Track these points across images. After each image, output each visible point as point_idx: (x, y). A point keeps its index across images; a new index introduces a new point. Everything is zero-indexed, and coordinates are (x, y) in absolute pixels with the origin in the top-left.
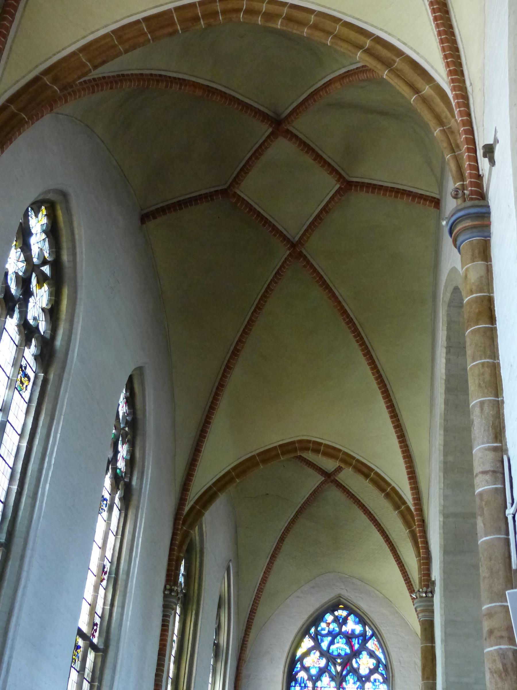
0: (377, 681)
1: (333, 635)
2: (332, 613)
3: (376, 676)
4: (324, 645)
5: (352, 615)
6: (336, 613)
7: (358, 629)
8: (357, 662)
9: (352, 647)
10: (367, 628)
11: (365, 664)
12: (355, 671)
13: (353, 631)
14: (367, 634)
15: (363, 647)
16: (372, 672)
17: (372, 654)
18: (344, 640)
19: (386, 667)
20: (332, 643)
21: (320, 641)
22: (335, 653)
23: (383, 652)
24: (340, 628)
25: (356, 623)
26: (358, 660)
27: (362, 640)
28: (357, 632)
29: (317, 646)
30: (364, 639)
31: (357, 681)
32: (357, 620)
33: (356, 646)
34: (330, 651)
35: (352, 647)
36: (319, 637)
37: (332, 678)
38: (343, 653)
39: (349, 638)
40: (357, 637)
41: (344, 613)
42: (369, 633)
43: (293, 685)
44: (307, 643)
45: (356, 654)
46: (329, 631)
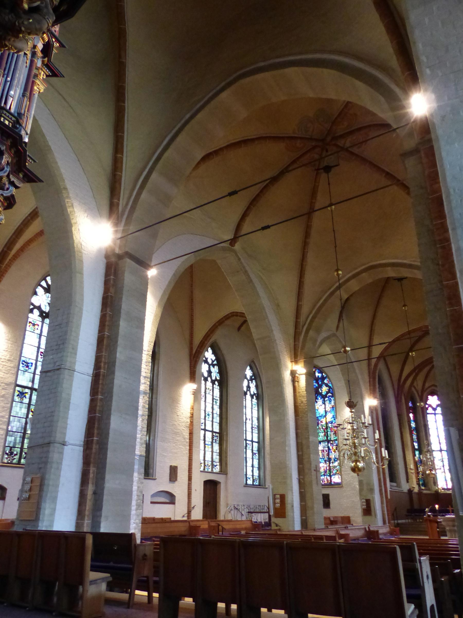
3: (330, 394)
10: (324, 374)
11: (324, 389)
12: (321, 394)
15: (323, 382)
16: (327, 393)
17: (327, 385)
30: (323, 378)
33: (320, 383)
45: (320, 386)
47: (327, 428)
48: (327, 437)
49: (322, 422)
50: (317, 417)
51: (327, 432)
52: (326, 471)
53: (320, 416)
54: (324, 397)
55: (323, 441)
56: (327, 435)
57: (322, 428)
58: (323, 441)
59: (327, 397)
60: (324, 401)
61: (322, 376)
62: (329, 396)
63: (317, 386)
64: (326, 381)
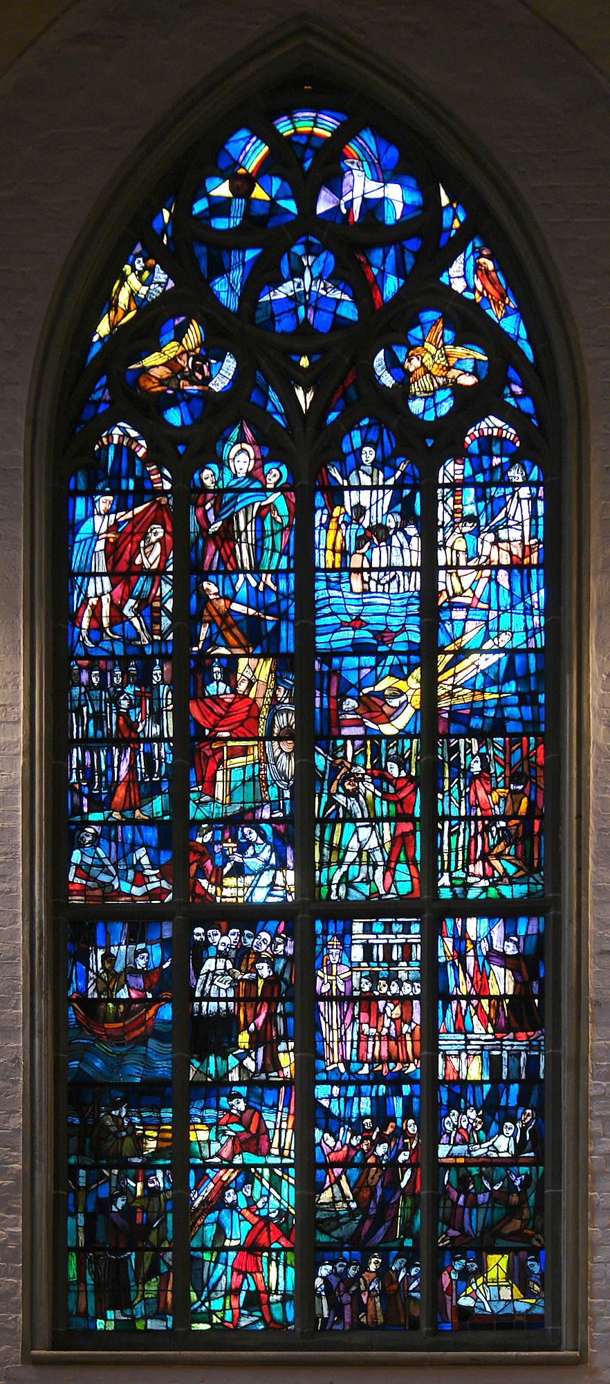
0: (496, 449)
1: (273, 239)
2: (268, 134)
3: (492, 424)
4: (225, 291)
5: (368, 138)
6: (284, 128)
7: (396, 197)
8: (393, 364)
9: (364, 289)
11: (437, 366)
13: (373, 207)
14: (447, 216)
15: (425, 288)
16: (470, 404)
17: (467, 322)
18: (326, 260)
19: (540, 378)
20: (264, 275)
21: (203, 265)
22: (285, 324)
23: (526, 313)
24: (307, 202)
25: (383, 175)
26: (401, 354)
27: (416, 255)
28: (394, 212)
29: (189, 299)
30: (425, 243)
31: (395, 455)
32: (393, 153)
34: (260, 316)
35: (364, 289)
36: (200, 250)
37: (272, 446)
38: (323, 322)
39: (352, 240)
40: (395, 236)
41: (326, 127)
42: (454, 221)
43: (82, 486)
44: (137, 284)
45: (390, 326)
46: (247, 216)
47: (429, 782)
48: (429, 872)
49: (374, 706)
50: (328, 656)
51: (432, 820)
52: (386, 1208)
53: (358, 649)
54: (418, 452)
55: (374, 909)
56: (433, 850)
57: (380, 775)
58: (374, 909)
59: (460, 454)
60: (429, 487)
61: (424, 217)
62: (486, 442)
63: (348, 311)
64: (457, 276)
